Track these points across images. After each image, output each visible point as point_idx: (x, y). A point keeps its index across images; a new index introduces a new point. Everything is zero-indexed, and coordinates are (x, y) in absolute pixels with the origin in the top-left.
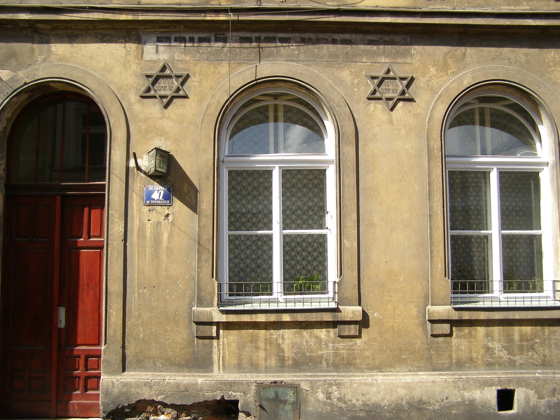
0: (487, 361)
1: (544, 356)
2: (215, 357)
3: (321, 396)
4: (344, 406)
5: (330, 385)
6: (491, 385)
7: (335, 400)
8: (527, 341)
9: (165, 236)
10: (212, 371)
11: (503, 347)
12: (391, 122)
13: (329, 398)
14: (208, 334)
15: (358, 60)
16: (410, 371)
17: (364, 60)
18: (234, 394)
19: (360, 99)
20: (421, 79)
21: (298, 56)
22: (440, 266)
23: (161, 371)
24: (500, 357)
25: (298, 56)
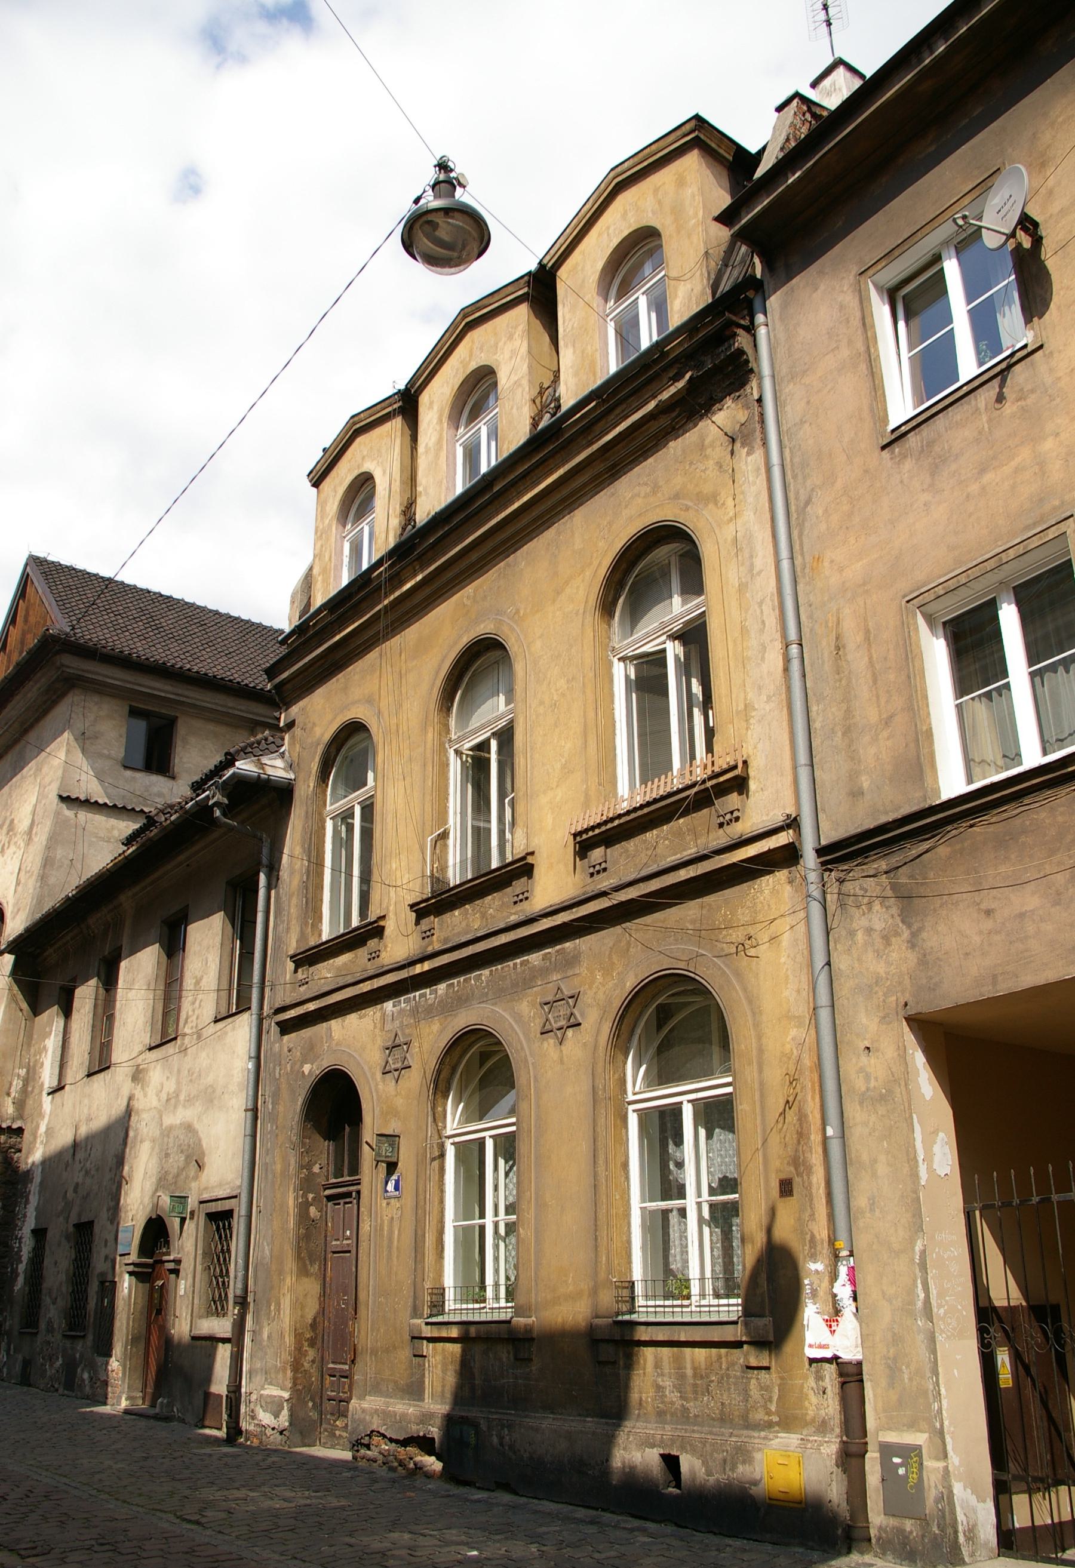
0: (658, 1407)
1: (723, 1404)
2: (427, 1383)
3: (495, 1440)
4: (514, 1457)
5: (503, 1426)
6: (653, 1446)
7: (507, 1448)
8: (702, 1377)
9: (396, 1232)
10: (423, 1400)
11: (674, 1386)
12: (562, 1062)
13: (501, 1444)
14: (420, 1354)
15: (534, 984)
16: (580, 1415)
17: (539, 983)
18: (432, 1429)
19: (535, 1037)
20: (589, 992)
21: (487, 994)
22: (604, 1259)
23: (391, 1397)
24: (672, 1403)
25: (487, 994)
